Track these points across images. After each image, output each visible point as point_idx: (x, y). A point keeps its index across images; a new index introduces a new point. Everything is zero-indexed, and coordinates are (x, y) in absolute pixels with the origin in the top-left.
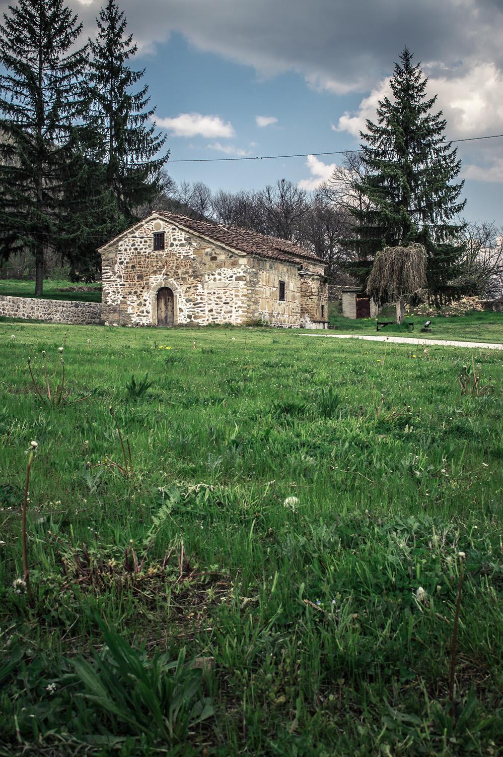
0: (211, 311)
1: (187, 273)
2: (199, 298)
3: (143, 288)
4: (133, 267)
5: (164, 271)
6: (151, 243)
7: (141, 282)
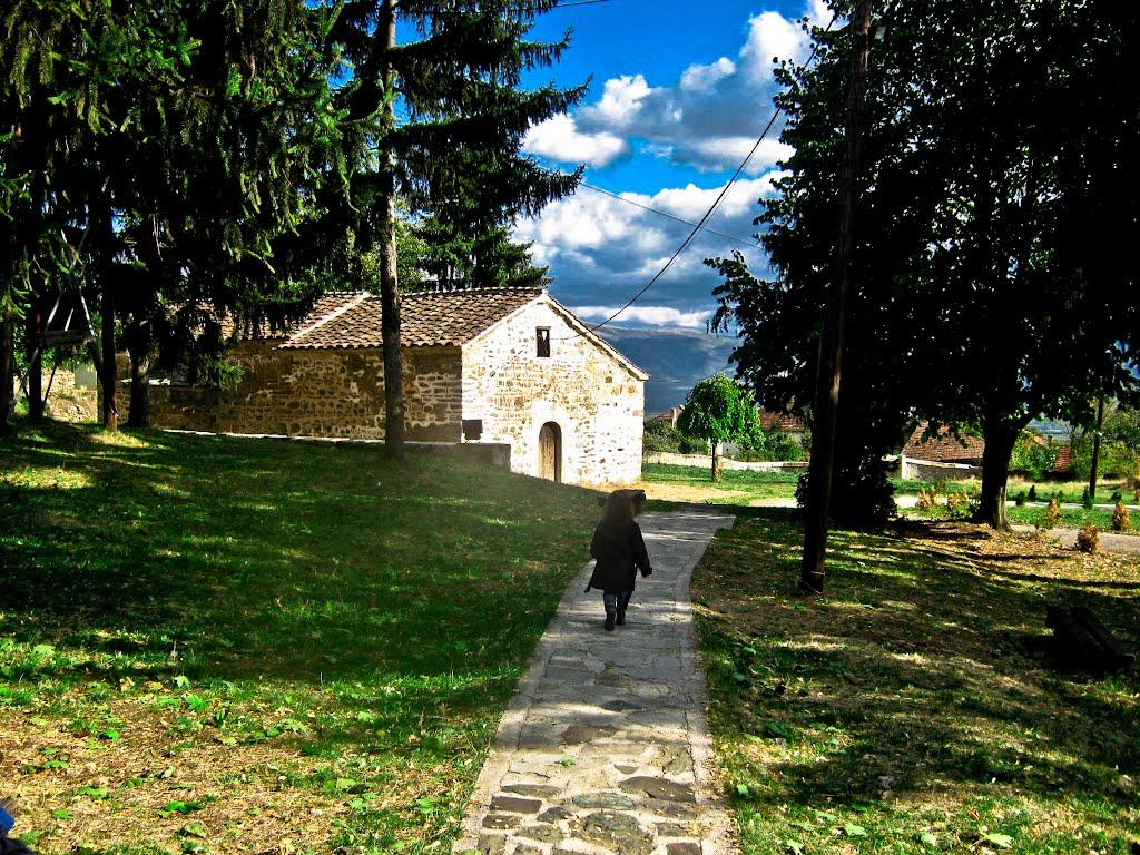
0: (603, 461)
1: (578, 400)
2: (590, 440)
3: (523, 422)
4: (509, 384)
5: (551, 395)
6: (534, 345)
7: (520, 412)
